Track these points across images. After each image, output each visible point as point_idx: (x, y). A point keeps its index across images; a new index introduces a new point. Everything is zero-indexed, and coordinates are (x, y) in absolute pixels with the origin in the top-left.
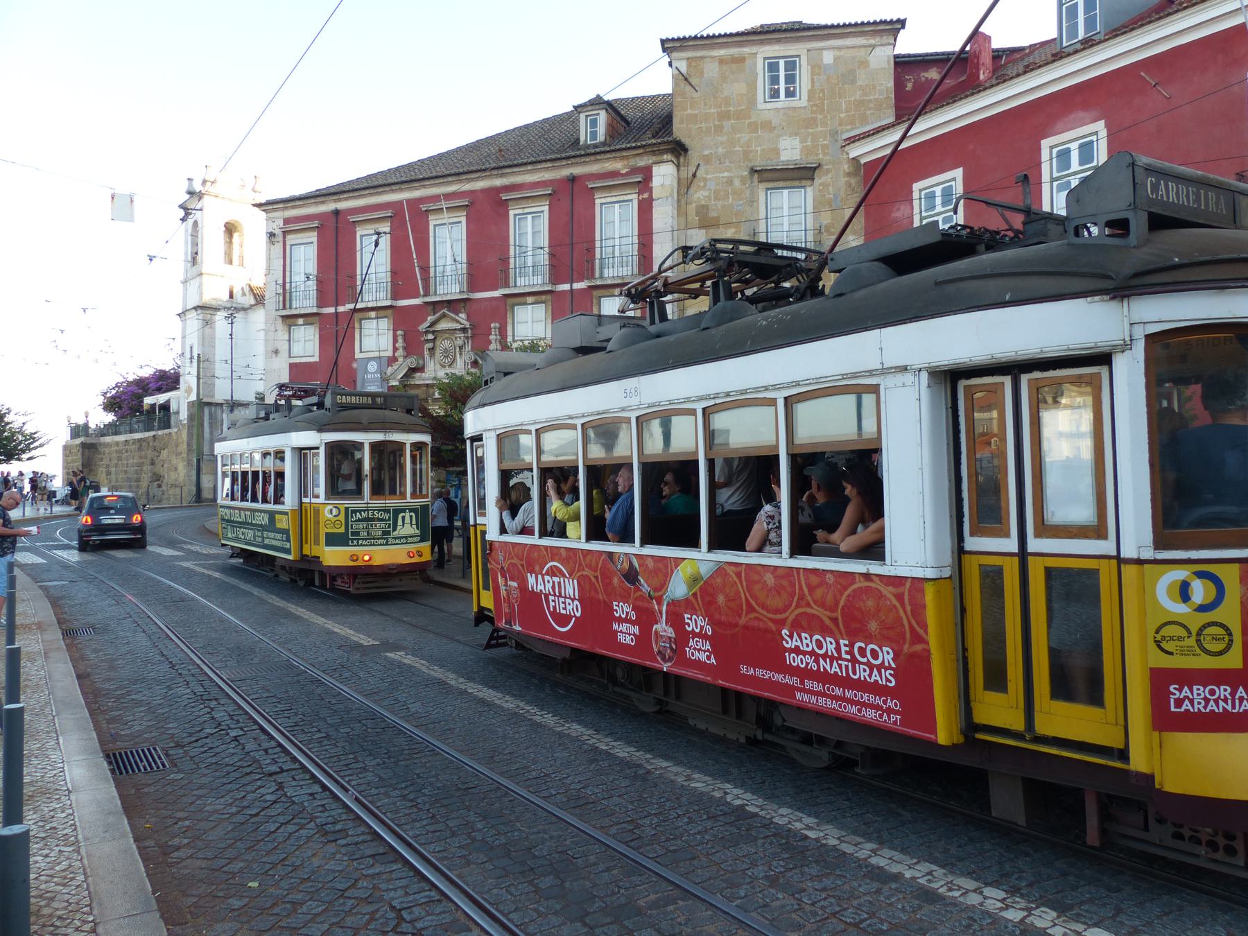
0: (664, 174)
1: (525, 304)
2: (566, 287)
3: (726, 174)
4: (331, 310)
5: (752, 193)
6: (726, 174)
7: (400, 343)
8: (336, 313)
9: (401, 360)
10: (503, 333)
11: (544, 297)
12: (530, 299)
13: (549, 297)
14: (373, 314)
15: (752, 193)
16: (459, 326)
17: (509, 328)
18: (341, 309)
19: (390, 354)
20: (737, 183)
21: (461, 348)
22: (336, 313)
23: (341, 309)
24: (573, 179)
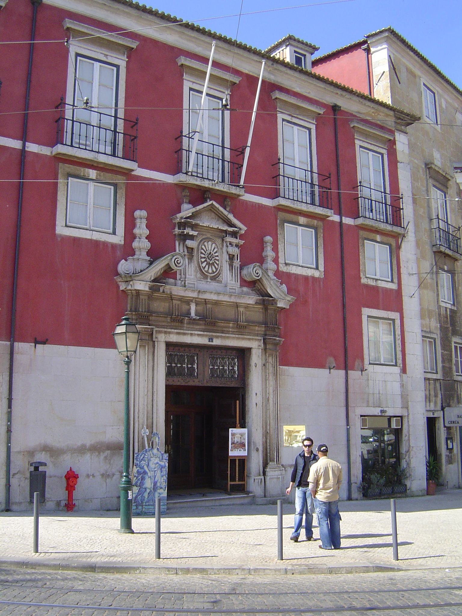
0: (402, 142)
1: (297, 223)
2: (336, 218)
3: (416, 161)
4: (16, 144)
5: (427, 185)
6: (416, 161)
7: (141, 230)
8: (23, 152)
9: (143, 255)
10: (275, 249)
11: (315, 222)
12: (302, 220)
13: (321, 223)
14: (93, 174)
15: (427, 185)
16: (231, 229)
17: (280, 247)
18: (32, 148)
19: (118, 239)
20: (421, 171)
21: (231, 258)
22: (23, 152)
23: (32, 148)
24: (335, 108)
